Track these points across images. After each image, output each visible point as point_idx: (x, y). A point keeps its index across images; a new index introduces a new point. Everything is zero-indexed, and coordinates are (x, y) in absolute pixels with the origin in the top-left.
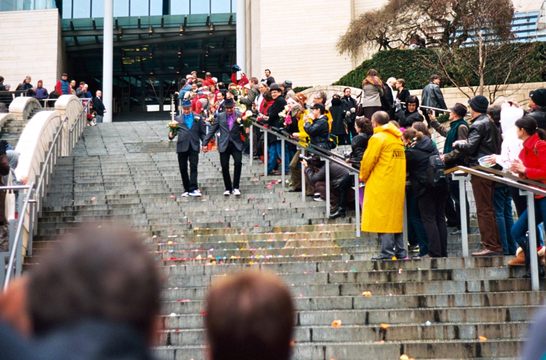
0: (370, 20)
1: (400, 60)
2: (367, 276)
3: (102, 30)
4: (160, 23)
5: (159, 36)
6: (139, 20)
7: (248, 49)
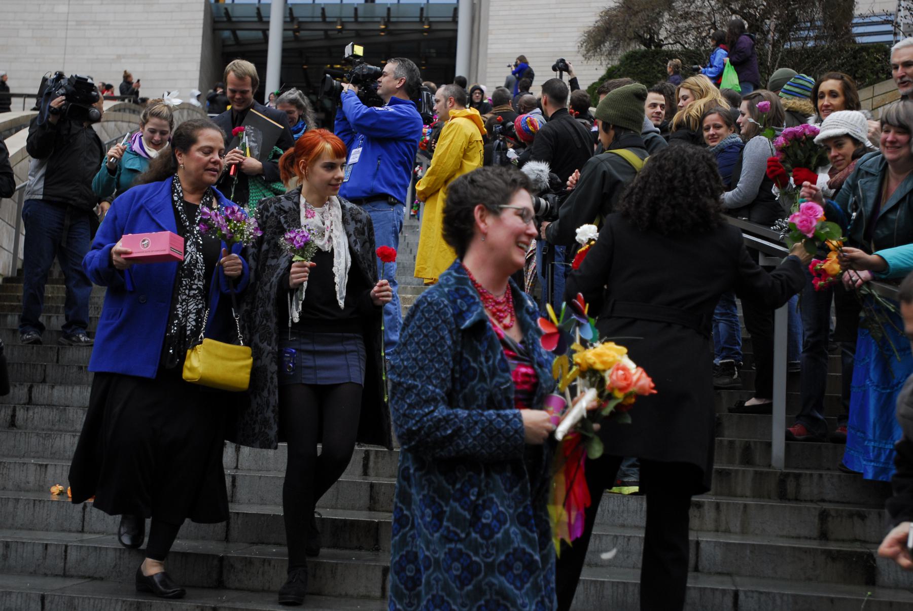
0: (629, 8)
1: (659, 66)
3: (268, 23)
4: (353, 15)
5: (353, 34)
6: (323, 9)
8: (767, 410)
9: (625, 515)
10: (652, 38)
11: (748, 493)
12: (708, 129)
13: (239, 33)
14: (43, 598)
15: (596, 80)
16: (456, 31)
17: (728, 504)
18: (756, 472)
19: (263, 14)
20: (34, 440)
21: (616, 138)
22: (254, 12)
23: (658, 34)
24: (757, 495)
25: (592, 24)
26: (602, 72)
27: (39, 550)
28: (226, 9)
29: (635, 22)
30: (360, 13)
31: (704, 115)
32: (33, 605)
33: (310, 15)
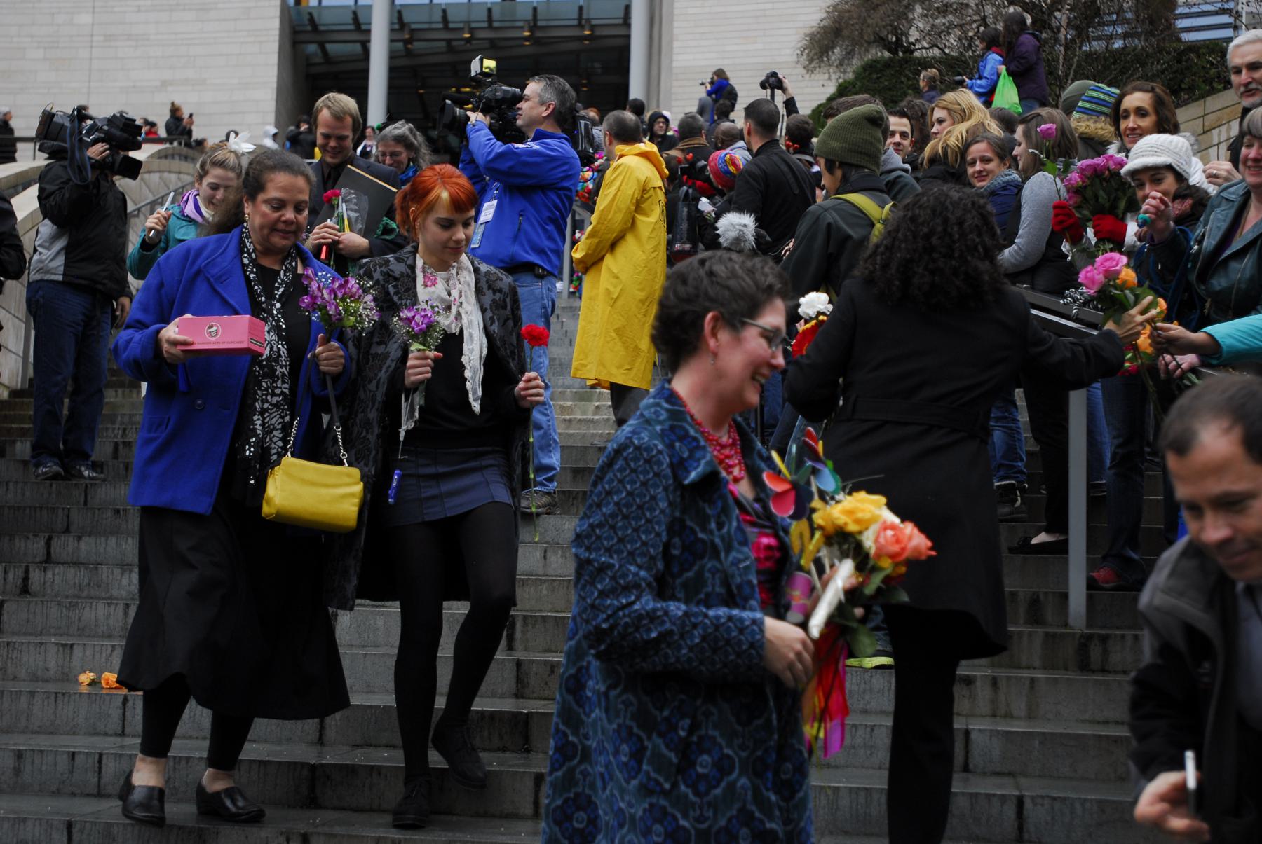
2: (569, 476)
3: (369, 31)
5: (486, 44)
6: (444, 11)
7: (654, 73)
8: (1060, 549)
9: (867, 697)
10: (899, 40)
11: (1037, 663)
12: (973, 163)
13: (329, 46)
14: (69, 826)
15: (823, 101)
16: (628, 37)
17: (1009, 678)
18: (1047, 634)
19: (362, 20)
20: (54, 610)
21: (845, 178)
22: (349, 18)
23: (907, 35)
24: (1050, 664)
25: (815, 24)
26: (831, 89)
27: (63, 762)
28: (310, 14)
29: (875, 18)
30: (496, 15)
31: (968, 145)
32: (55, 836)
33: (426, 19)
